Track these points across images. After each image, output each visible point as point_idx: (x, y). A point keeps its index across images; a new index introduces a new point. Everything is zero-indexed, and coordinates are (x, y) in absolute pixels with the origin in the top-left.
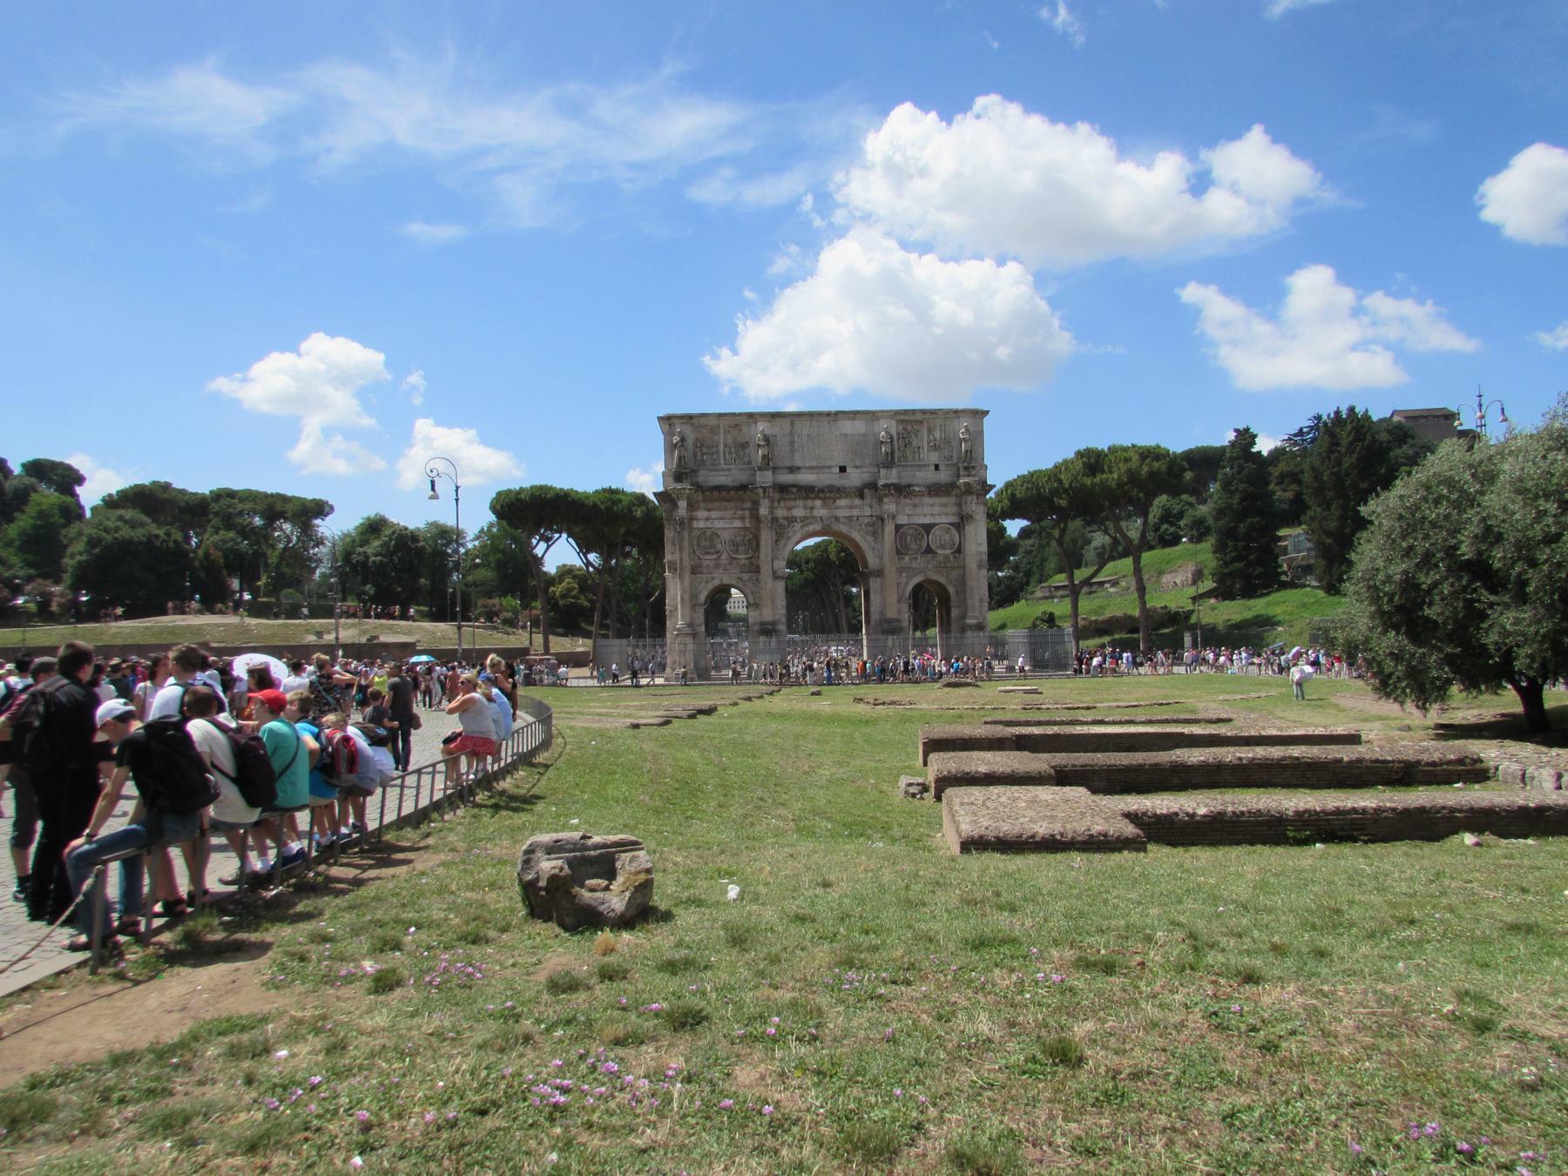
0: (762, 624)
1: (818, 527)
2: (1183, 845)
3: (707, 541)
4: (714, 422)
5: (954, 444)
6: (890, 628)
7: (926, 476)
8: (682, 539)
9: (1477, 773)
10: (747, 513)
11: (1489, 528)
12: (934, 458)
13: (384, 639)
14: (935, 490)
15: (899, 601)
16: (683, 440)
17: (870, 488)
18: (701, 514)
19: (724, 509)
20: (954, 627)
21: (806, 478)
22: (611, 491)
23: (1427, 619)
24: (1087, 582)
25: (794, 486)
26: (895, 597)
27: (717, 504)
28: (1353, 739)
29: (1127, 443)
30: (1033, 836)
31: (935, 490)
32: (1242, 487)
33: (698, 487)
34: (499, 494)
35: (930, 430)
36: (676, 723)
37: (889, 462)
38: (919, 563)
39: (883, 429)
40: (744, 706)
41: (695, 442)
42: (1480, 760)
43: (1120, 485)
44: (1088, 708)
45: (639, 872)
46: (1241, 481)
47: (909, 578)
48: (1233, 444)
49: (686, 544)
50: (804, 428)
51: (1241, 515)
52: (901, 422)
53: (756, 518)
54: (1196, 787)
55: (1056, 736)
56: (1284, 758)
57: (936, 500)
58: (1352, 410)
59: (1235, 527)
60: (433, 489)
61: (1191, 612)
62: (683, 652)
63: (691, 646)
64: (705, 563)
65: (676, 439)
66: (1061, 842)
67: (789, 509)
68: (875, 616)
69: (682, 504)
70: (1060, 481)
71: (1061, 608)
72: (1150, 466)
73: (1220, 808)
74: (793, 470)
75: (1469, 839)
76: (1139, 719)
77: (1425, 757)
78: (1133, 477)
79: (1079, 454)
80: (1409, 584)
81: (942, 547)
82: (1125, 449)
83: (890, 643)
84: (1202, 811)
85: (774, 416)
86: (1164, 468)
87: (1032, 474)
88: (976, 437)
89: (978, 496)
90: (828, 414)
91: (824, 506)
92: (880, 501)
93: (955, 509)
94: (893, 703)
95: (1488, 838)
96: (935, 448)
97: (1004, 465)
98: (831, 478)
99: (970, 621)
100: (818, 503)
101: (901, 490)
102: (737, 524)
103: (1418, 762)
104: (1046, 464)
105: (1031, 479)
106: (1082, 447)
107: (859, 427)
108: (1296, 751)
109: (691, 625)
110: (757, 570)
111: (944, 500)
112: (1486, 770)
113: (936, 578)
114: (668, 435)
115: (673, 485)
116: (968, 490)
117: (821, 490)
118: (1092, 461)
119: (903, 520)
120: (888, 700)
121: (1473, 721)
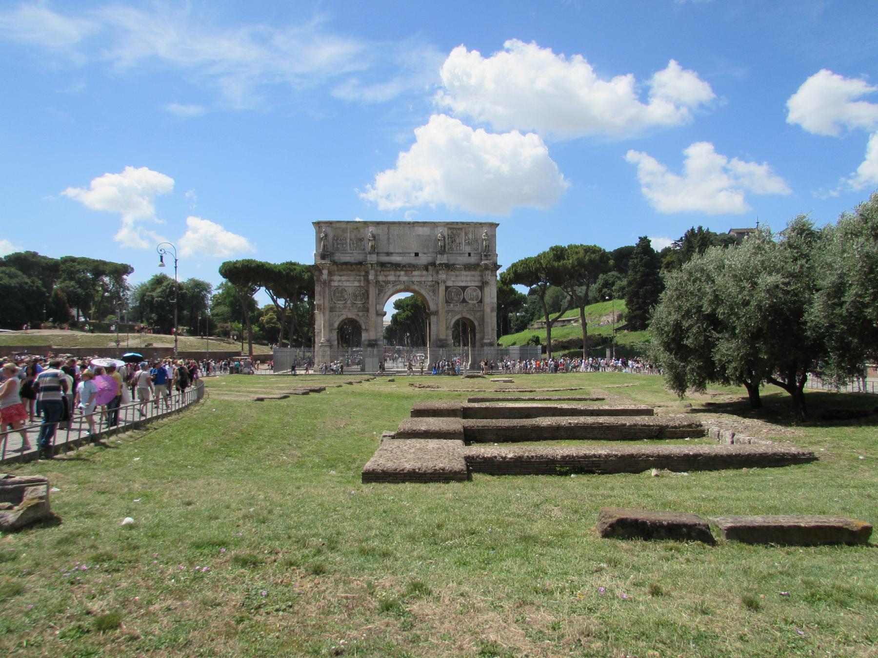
0: (369, 341)
1: (402, 287)
2: (498, 475)
3: (340, 293)
4: (344, 226)
5: (480, 242)
6: (441, 344)
7: (464, 259)
8: (324, 292)
9: (697, 432)
10: (362, 278)
11: (717, 296)
12: (468, 249)
13: (155, 345)
14: (468, 267)
15: (447, 329)
16: (326, 236)
17: (431, 266)
18: (336, 278)
19: (350, 275)
20: (478, 344)
21: (396, 259)
22: (291, 264)
23: (686, 346)
24: (555, 320)
25: (389, 263)
26: (444, 326)
28: (649, 412)
29: (578, 244)
30: (403, 470)
31: (468, 267)
32: (641, 269)
33: (334, 263)
34: (224, 264)
35: (466, 234)
36: (292, 397)
37: (443, 251)
38: (459, 308)
39: (439, 232)
40: (346, 387)
41: (332, 237)
42: (701, 426)
43: (573, 267)
44: (531, 391)
45: (34, 499)
46: (642, 266)
47: (453, 316)
48: (638, 245)
49: (327, 295)
50: (395, 231)
51: (641, 284)
52: (450, 228)
53: (367, 281)
54: (545, 439)
55: (487, 409)
56: (594, 423)
57: (467, 273)
58: (700, 228)
59: (638, 291)
60: (162, 261)
61: (611, 339)
62: (324, 356)
63: (329, 353)
64: (338, 306)
65: (322, 235)
66: (418, 473)
67: (386, 276)
68: (433, 337)
69: (325, 272)
70: (541, 264)
71: (542, 334)
72: (589, 256)
73: (521, 454)
74: (388, 254)
75: (654, 472)
76: (554, 398)
77: (671, 424)
78: (580, 262)
79: (552, 249)
80: (677, 326)
81: (472, 299)
82: (576, 247)
83: (441, 352)
84: (510, 455)
85: (378, 224)
86: (597, 258)
87: (526, 260)
88: (492, 238)
89: (492, 271)
90: (409, 223)
91: (406, 275)
92: (437, 273)
93: (478, 278)
94: (429, 387)
95: (666, 472)
96: (469, 244)
97: (508, 256)
98: (410, 259)
99: (485, 341)
100: (402, 273)
101: (449, 267)
102: (357, 284)
103: (667, 426)
104: (533, 254)
105: (526, 262)
106: (554, 245)
107: (425, 231)
108: (601, 419)
109: (329, 341)
110: (368, 311)
111: (474, 273)
112: (704, 431)
113: (468, 316)
114: (318, 232)
115: (320, 261)
116: (486, 268)
117: (404, 266)
118: (559, 253)
119: (450, 284)
120: (426, 385)
121: (727, 401)
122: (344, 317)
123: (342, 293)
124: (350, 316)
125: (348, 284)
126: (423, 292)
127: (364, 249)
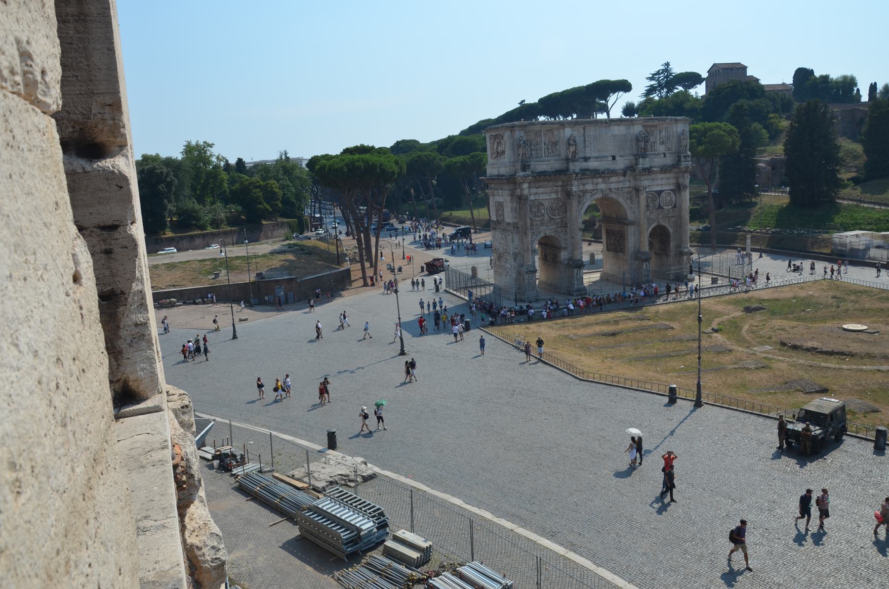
7: (658, 161)
10: (560, 189)
12: (661, 149)
14: (664, 169)
18: (534, 190)
21: (593, 164)
25: (587, 170)
27: (541, 184)
31: (664, 169)
67: (584, 185)
74: (586, 159)
91: (603, 182)
93: (673, 181)
96: (662, 143)
100: (600, 180)
102: (554, 196)
111: (668, 175)
117: (603, 172)
122: (542, 235)
124: (548, 233)
126: (621, 200)
127: (559, 155)
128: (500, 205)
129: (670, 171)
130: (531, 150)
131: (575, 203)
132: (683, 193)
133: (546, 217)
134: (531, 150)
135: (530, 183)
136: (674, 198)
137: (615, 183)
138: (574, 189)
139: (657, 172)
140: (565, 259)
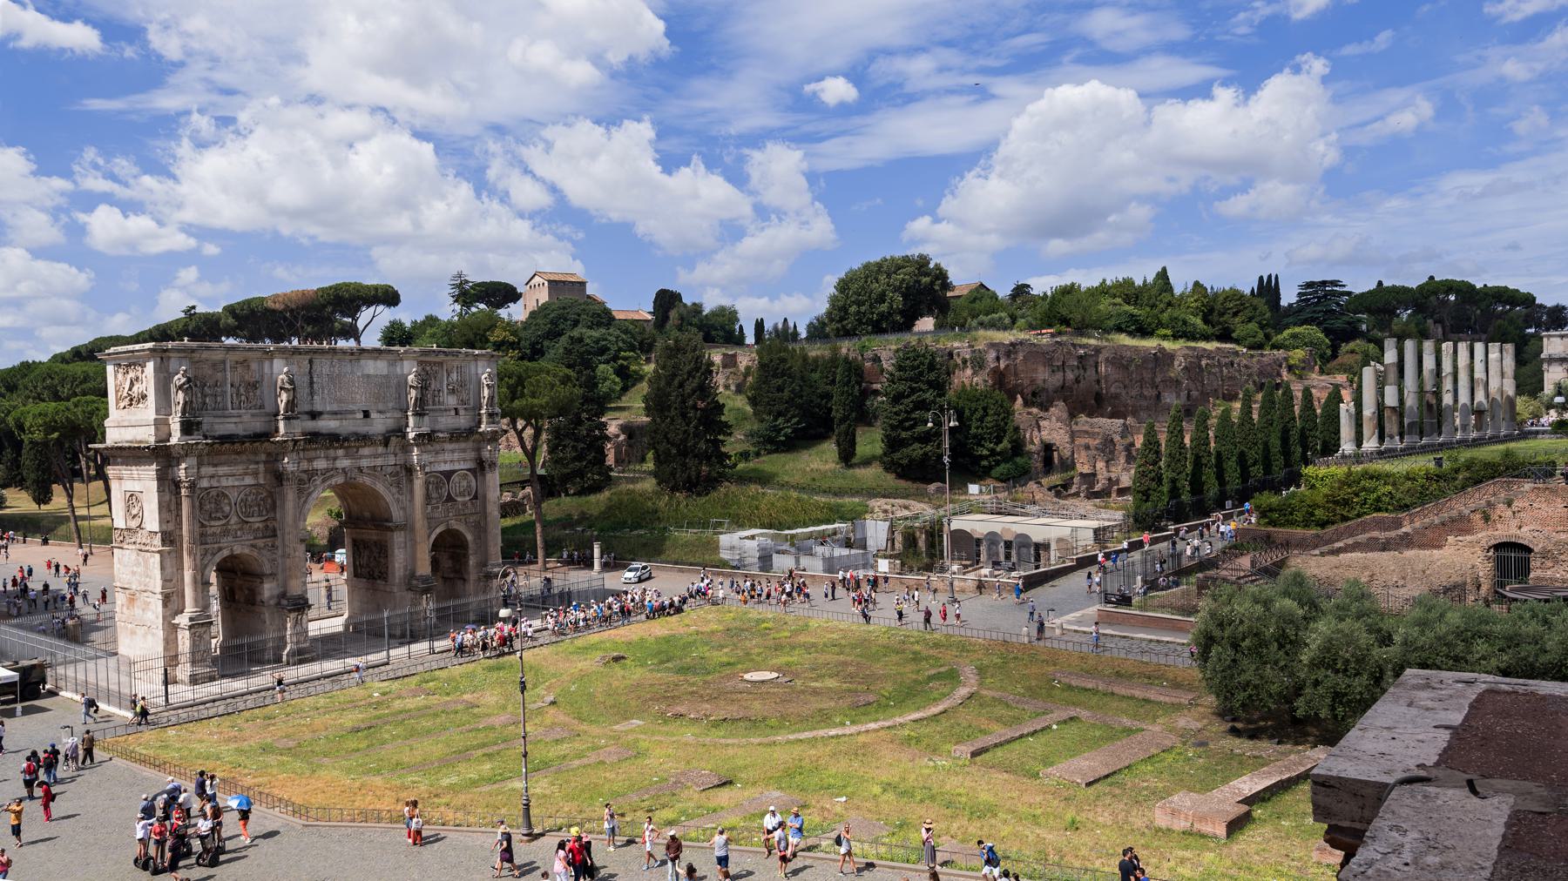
10: (261, 467)
14: (456, 436)
21: (327, 425)
27: (224, 458)
67: (310, 460)
74: (314, 415)
81: (462, 494)
91: (347, 456)
93: (471, 455)
96: (452, 392)
100: (340, 452)
102: (249, 480)
111: (463, 445)
117: (346, 439)
122: (226, 553)
123: (217, 503)
124: (238, 550)
125: (230, 482)
126: (380, 488)
128: (132, 498)
129: (467, 439)
130: (204, 396)
131: (290, 494)
132: (489, 476)
133: (234, 520)
134: (204, 396)
135: (199, 456)
136: (473, 484)
137: (368, 457)
138: (291, 468)
139: (443, 440)
140: (271, 598)
